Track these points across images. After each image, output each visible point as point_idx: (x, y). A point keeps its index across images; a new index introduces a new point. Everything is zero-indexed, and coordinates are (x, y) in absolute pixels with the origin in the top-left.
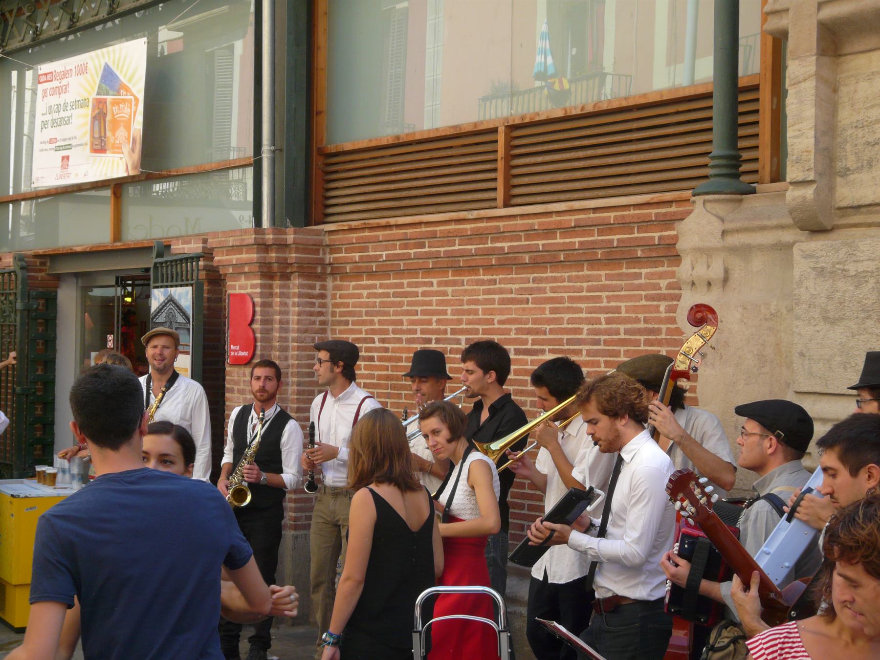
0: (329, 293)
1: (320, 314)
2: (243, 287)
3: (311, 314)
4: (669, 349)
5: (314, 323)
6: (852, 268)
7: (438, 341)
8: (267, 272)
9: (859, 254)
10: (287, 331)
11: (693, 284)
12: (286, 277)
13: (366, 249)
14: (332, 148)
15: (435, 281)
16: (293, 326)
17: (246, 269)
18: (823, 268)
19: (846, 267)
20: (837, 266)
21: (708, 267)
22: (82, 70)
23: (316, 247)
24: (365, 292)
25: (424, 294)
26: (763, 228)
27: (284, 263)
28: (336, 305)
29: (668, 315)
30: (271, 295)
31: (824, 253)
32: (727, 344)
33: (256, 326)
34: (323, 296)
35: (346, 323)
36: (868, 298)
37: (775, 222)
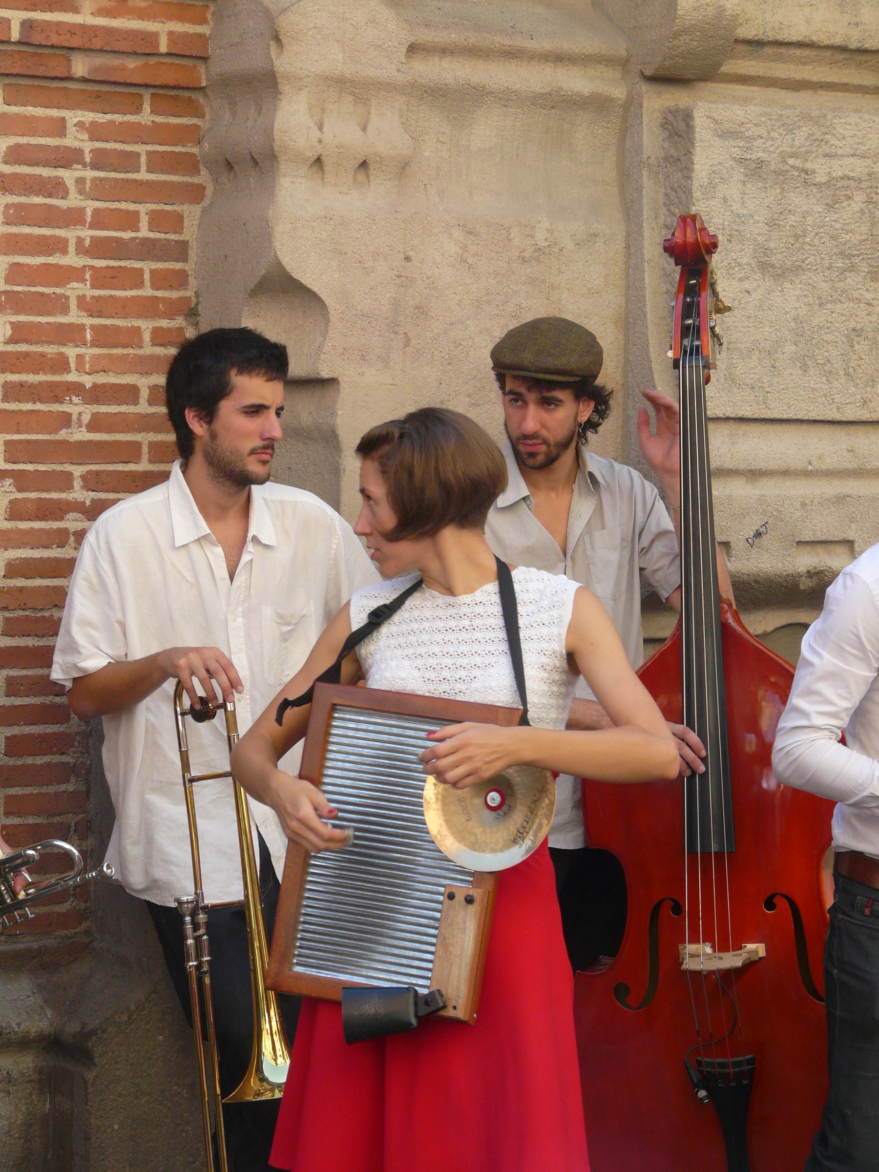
4: (22, 318)
6: (821, 169)
9: (836, 142)
11: (318, 161)
18: (760, 163)
19: (808, 166)
20: (791, 161)
21: (364, 129)
26: (512, 54)
29: (14, 230)
31: (762, 131)
32: (421, 310)
36: (851, 231)
37: (547, 45)
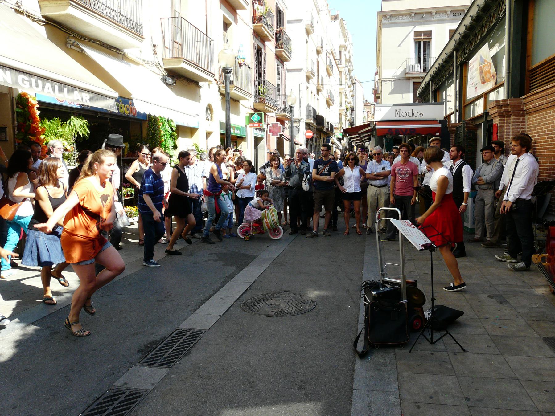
0: (526, 121)
1: (522, 128)
2: (497, 121)
3: (518, 128)
5: (519, 132)
7: (551, 134)
8: (502, 115)
10: (509, 135)
12: (510, 116)
13: (533, 103)
14: (530, 68)
15: (551, 111)
16: (511, 133)
17: (496, 115)
22: (476, 59)
23: (520, 104)
24: (535, 119)
25: (549, 117)
27: (507, 111)
28: (528, 125)
30: (504, 123)
33: (498, 134)
34: (524, 122)
35: (530, 131)
